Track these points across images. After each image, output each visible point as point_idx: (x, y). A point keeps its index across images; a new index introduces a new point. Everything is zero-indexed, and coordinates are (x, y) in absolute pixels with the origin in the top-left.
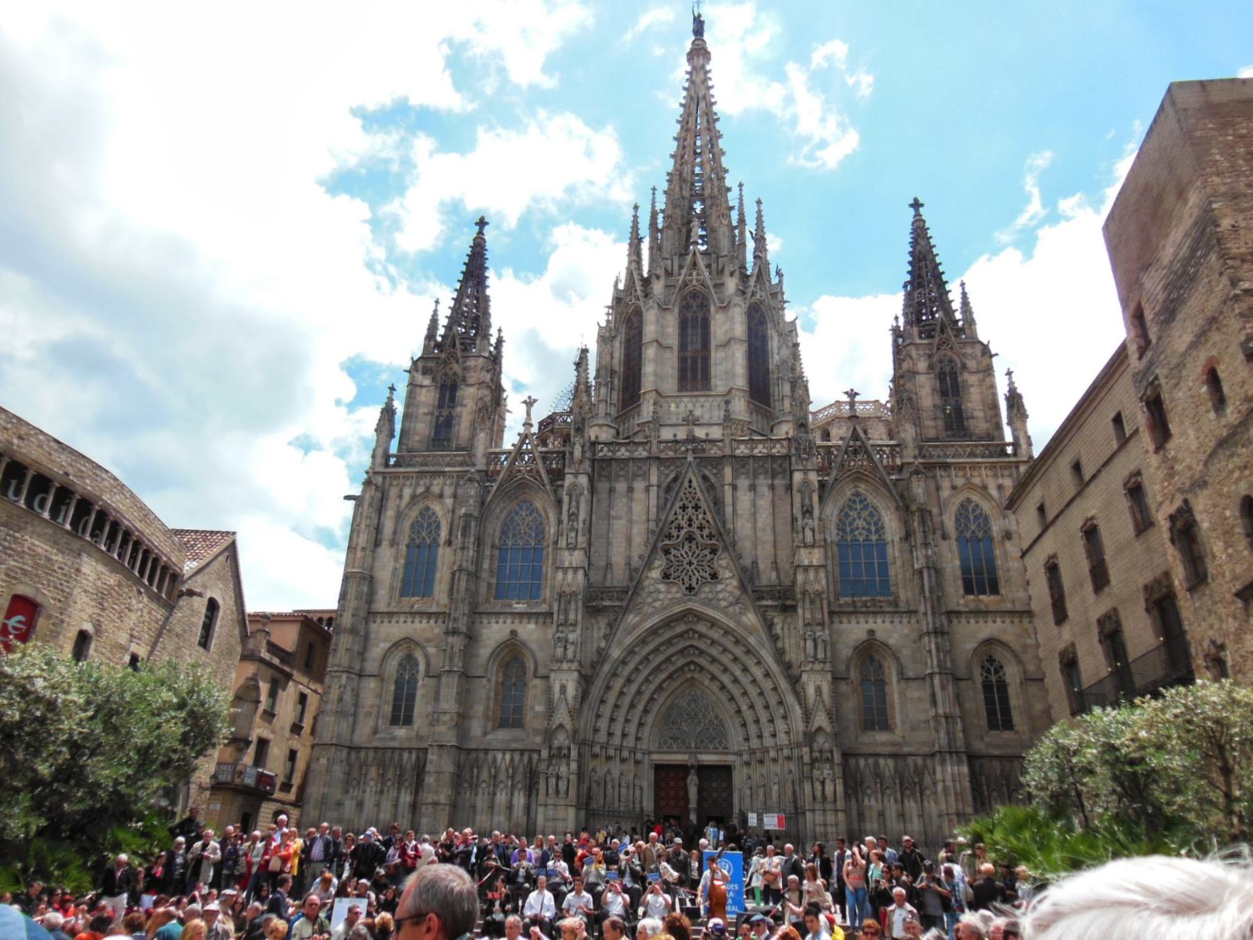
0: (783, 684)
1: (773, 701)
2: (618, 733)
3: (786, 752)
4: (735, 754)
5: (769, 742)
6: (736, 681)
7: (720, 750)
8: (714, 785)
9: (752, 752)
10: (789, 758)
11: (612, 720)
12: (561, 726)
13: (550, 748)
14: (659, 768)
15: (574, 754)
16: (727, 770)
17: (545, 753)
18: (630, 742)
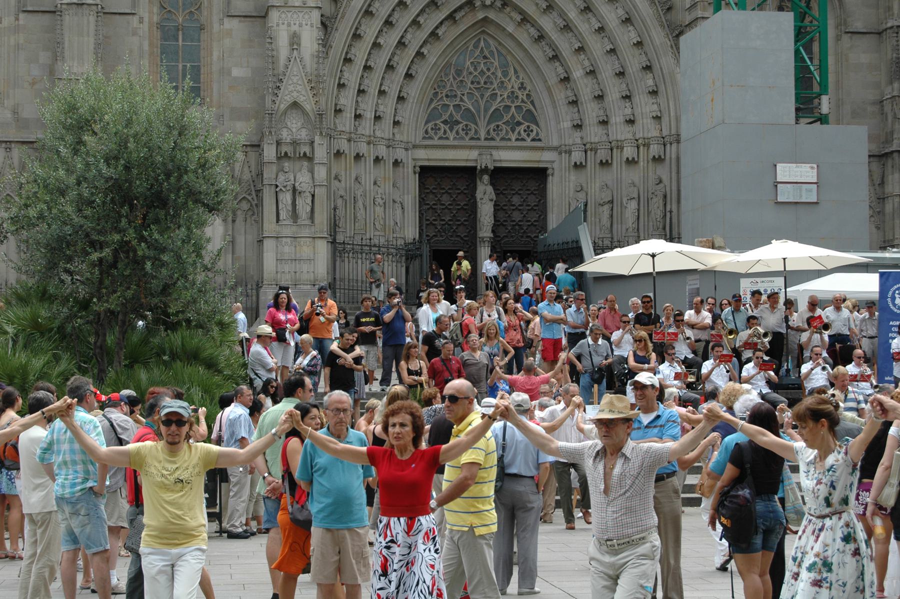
0: (658, 37)
1: (634, 61)
2: (369, 115)
3: (655, 150)
4: (555, 149)
5: (619, 131)
6: (567, 28)
7: (528, 143)
8: (516, 200)
9: (588, 149)
10: (658, 160)
11: (361, 92)
12: (295, 105)
13: (278, 143)
14: (426, 173)
15: (321, 153)
16: (540, 174)
17: (269, 152)
18: (385, 130)
